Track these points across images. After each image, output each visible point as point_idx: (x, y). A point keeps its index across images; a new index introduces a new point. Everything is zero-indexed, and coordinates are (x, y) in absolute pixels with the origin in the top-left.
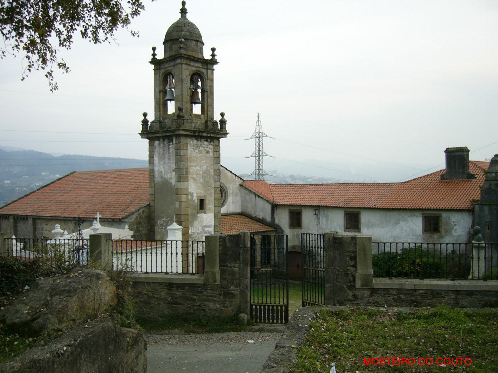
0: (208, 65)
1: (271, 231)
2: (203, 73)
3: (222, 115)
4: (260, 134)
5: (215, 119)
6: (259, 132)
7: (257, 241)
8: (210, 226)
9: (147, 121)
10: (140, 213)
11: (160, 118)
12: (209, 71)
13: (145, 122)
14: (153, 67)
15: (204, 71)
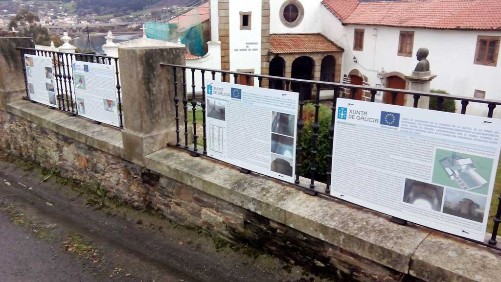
8: (257, 44)
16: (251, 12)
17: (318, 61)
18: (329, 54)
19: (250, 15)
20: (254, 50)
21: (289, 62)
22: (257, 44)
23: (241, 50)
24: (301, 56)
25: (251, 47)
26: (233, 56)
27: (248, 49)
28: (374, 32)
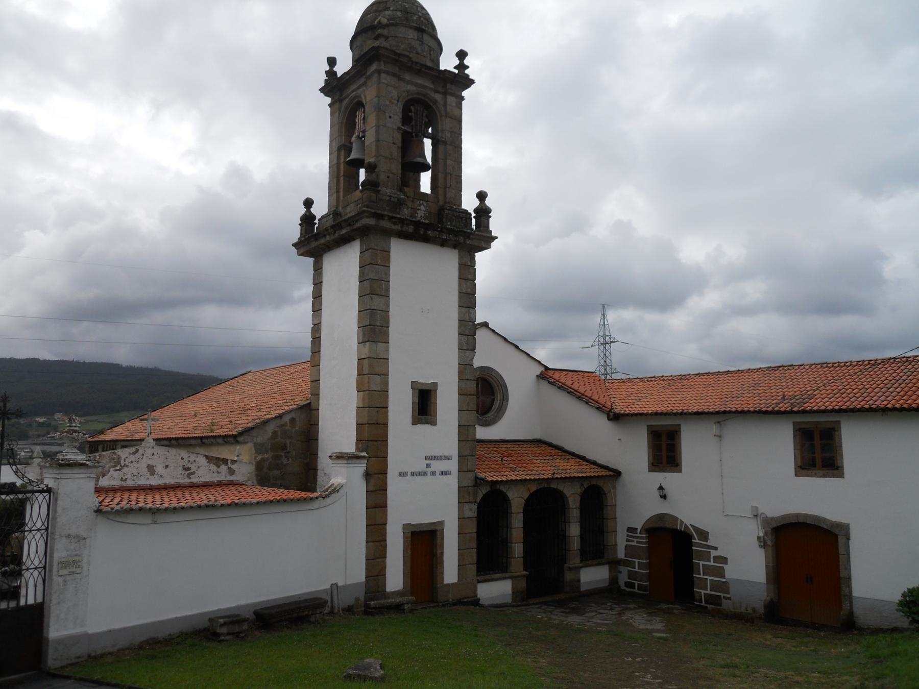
0: (448, 86)
1: (606, 476)
2: (435, 102)
3: (482, 196)
4: (607, 338)
5: (464, 207)
6: (605, 336)
7: (570, 500)
8: (448, 458)
9: (314, 217)
10: (285, 424)
11: (337, 207)
12: (451, 100)
13: (307, 220)
14: (328, 100)
15: (438, 97)
16: (436, 384)
17: (573, 496)
18: (594, 482)
19: (436, 391)
20: (442, 473)
21: (517, 499)
22: (448, 458)
25: (437, 466)
26: (395, 487)
27: (429, 470)
28: (714, 429)
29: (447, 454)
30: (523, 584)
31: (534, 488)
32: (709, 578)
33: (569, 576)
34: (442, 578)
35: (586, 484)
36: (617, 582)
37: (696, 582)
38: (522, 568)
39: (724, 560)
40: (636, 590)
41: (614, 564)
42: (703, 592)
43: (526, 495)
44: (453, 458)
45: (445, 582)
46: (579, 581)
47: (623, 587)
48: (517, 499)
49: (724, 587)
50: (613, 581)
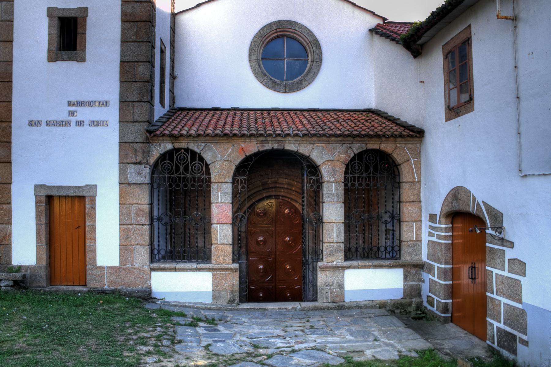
7: (325, 171)
8: (105, 104)
18: (373, 145)
20: (93, 124)
21: (222, 162)
22: (105, 104)
23: (48, 123)
24: (268, 147)
25: (84, 114)
27: (73, 119)
29: (102, 99)
30: (233, 281)
31: (253, 147)
32: (504, 300)
33: (322, 278)
34: (94, 258)
35: (357, 147)
36: (420, 295)
37: (490, 305)
38: (229, 259)
39: (519, 266)
40: (434, 309)
41: (414, 269)
42: (496, 324)
43: (239, 158)
44: (111, 103)
45: (99, 264)
46: (341, 286)
47: (425, 304)
48: (222, 162)
49: (518, 318)
50: (413, 292)
